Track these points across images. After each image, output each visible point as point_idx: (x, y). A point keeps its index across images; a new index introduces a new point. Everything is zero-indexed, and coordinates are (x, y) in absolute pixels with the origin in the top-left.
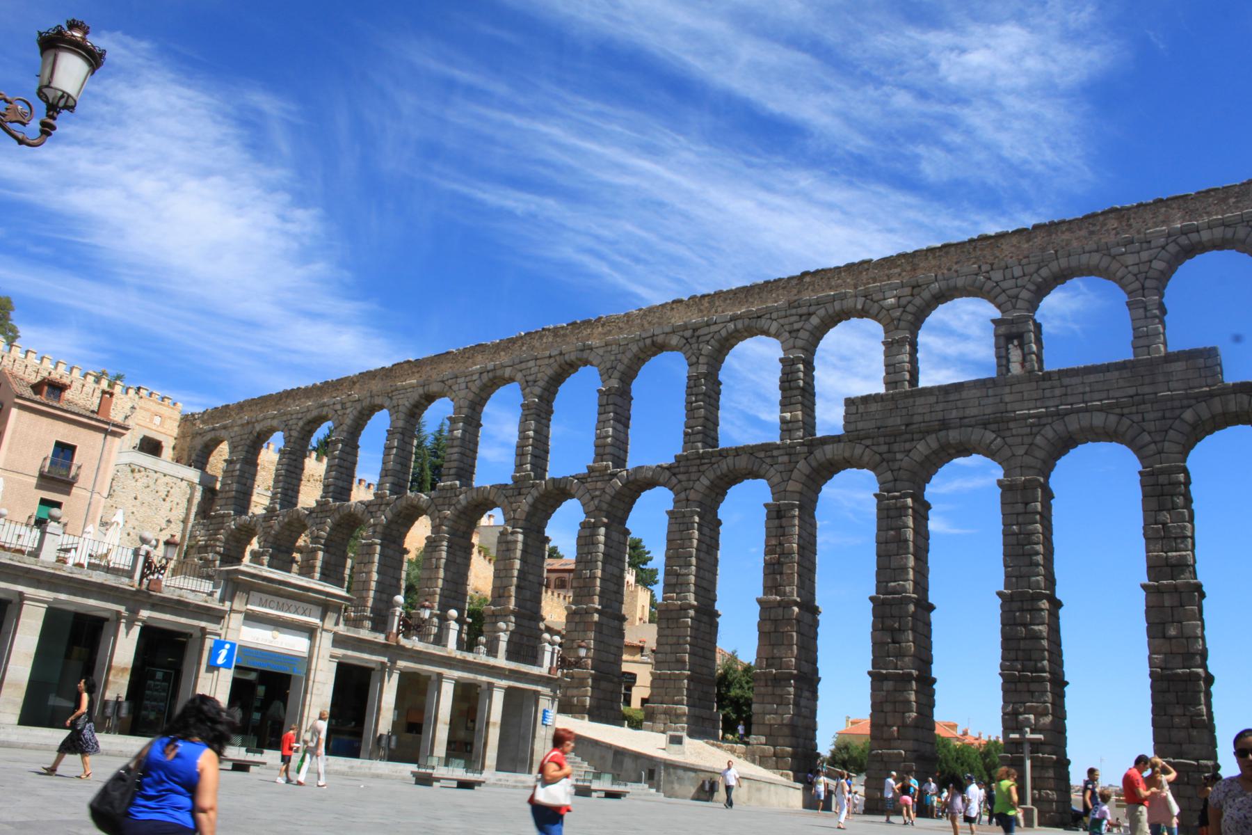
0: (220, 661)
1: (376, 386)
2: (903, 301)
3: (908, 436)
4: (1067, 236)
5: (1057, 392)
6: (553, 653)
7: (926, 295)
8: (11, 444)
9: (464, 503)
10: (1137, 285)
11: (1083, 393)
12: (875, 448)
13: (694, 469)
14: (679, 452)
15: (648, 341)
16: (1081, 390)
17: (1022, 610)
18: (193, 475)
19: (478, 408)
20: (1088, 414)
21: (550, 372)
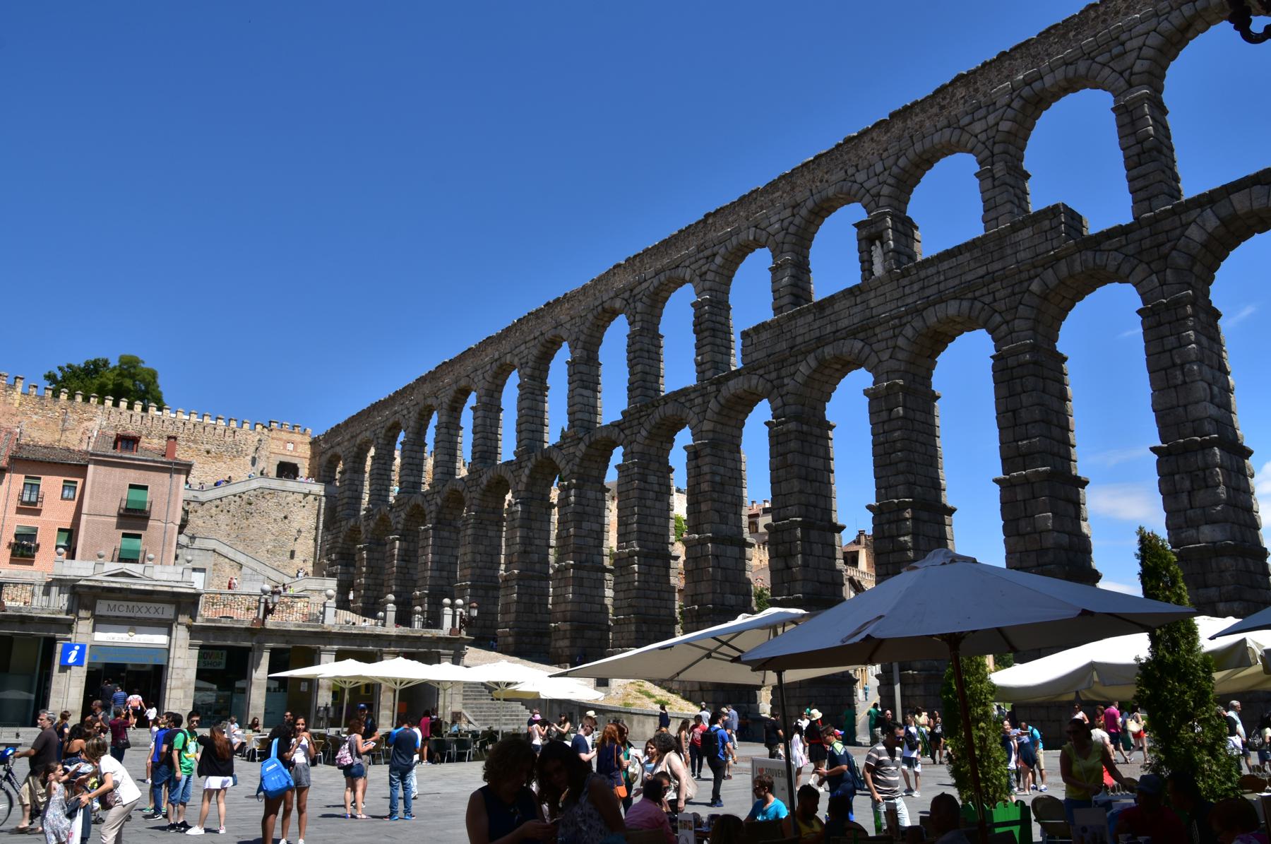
0: (71, 660)
1: (427, 388)
2: (786, 223)
3: (792, 359)
4: (921, 117)
5: (916, 287)
6: (454, 616)
7: (804, 212)
8: (92, 493)
9: (485, 482)
10: (987, 153)
11: (939, 283)
12: (767, 376)
13: (635, 422)
14: (625, 407)
15: (600, 308)
16: (936, 280)
17: (889, 522)
18: (319, 489)
19: (496, 395)
20: (944, 305)
21: (535, 352)
